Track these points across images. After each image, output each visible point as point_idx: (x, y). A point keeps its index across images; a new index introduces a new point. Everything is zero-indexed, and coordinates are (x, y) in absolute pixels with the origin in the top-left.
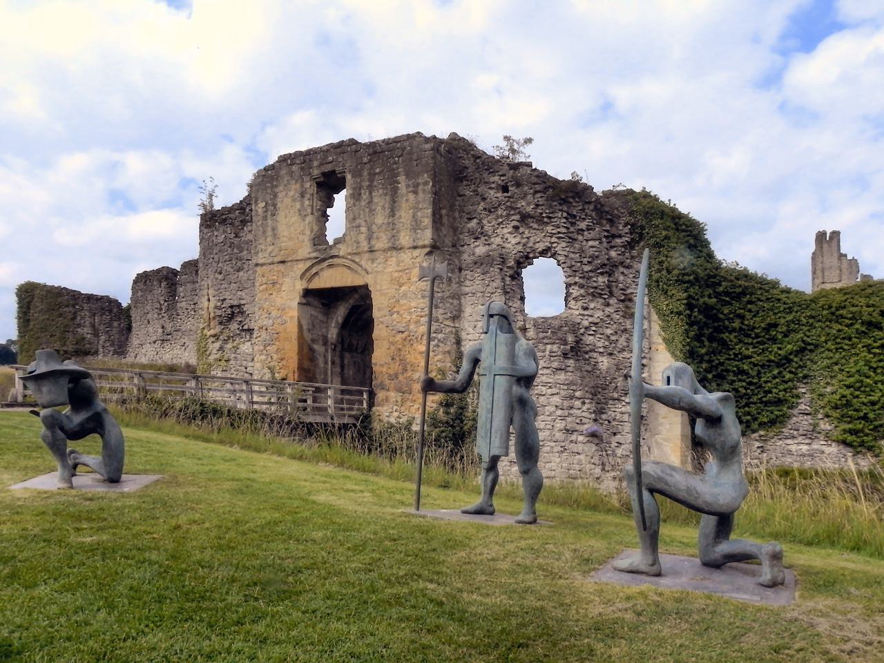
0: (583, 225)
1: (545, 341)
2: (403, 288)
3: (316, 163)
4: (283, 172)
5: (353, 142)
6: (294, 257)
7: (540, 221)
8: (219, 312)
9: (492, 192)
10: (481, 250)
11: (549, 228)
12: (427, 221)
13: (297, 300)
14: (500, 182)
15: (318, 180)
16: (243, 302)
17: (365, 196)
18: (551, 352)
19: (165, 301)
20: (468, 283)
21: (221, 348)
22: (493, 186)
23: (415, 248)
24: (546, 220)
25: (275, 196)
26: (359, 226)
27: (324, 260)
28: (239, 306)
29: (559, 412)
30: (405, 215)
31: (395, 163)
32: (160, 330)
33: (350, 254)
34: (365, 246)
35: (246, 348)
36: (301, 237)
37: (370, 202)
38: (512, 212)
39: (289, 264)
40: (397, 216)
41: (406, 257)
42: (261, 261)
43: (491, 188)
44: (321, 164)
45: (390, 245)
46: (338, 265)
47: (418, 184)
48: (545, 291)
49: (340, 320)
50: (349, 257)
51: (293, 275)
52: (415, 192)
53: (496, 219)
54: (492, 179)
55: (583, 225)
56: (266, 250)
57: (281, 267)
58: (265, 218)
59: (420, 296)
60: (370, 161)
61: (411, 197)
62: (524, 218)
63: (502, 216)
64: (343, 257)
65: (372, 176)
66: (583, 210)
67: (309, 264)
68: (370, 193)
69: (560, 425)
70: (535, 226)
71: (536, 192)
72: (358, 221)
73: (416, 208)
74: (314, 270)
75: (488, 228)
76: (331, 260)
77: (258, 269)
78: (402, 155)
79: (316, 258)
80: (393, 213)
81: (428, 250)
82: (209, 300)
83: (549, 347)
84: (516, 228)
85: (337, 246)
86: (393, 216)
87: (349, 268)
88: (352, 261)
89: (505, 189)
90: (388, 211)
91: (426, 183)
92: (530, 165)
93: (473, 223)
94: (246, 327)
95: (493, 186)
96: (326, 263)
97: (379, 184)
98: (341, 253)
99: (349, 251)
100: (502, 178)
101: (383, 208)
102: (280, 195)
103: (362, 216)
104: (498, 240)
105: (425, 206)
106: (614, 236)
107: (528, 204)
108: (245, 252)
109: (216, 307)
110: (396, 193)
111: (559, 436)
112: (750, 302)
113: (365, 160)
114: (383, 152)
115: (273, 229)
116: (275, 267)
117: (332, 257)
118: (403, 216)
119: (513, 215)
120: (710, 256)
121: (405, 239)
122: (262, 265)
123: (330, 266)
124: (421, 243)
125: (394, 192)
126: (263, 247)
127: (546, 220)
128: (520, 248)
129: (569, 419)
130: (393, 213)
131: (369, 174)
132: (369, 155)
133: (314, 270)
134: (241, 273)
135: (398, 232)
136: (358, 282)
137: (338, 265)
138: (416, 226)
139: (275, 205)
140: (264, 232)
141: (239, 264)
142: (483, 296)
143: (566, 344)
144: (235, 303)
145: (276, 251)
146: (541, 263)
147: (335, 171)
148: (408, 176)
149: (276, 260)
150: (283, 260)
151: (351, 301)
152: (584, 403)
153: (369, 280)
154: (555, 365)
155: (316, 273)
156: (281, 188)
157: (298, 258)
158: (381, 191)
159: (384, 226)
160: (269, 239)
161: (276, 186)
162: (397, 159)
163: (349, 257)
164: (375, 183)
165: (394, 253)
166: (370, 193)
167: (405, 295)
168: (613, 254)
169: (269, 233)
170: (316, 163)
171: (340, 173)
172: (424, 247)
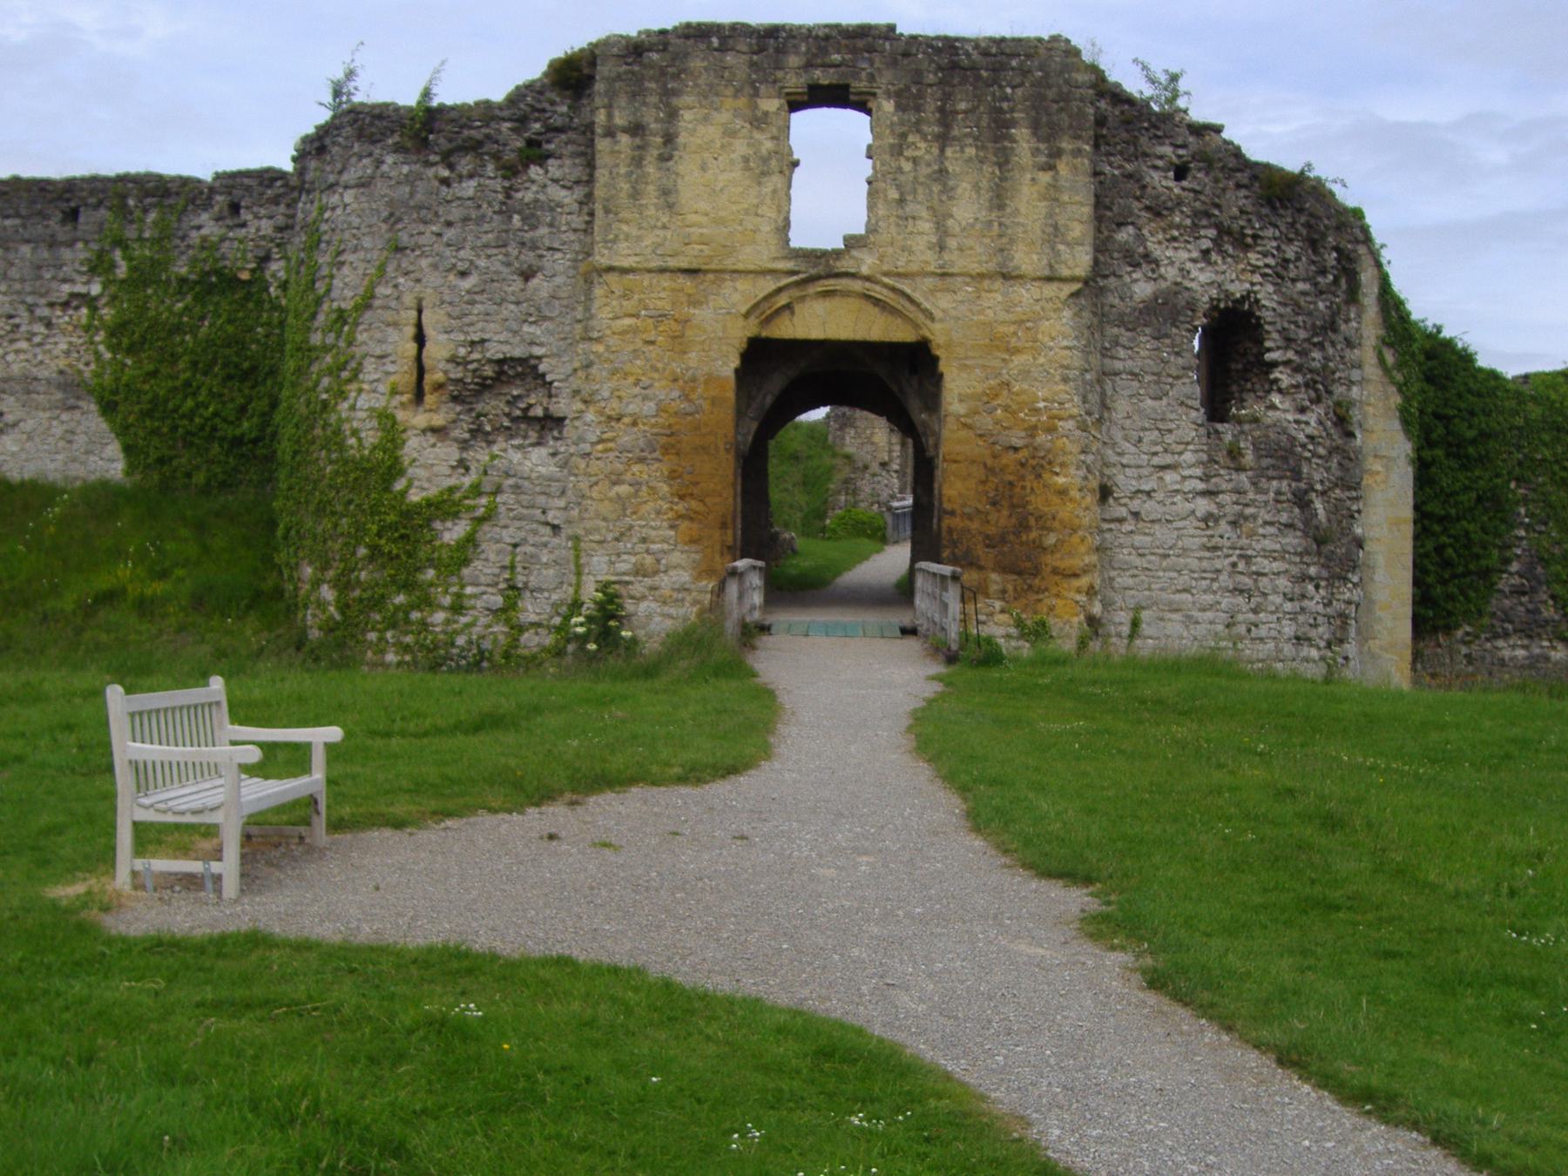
1: (1271, 473)
2: (1018, 360)
4: (697, 63)
6: (729, 263)
8: (457, 373)
9: (1156, 175)
14: (1174, 159)
15: (792, 98)
16: (537, 351)
18: (1278, 493)
20: (1122, 353)
22: (1160, 163)
23: (1049, 279)
24: (1249, 240)
25: (673, 114)
28: (522, 361)
29: (1288, 606)
31: (1006, 98)
33: (886, 274)
38: (1204, 222)
39: (711, 276)
40: (1008, 210)
41: (1026, 294)
43: (1155, 168)
45: (992, 266)
46: (846, 294)
49: (769, 400)
50: (886, 280)
51: (722, 303)
53: (1164, 230)
56: (639, 239)
57: (686, 283)
59: (1058, 378)
60: (941, 82)
63: (1178, 227)
64: (868, 279)
65: (946, 117)
66: (1292, 225)
67: (769, 285)
68: (942, 151)
69: (1289, 629)
70: (1231, 250)
73: (1052, 195)
74: (782, 300)
76: (831, 281)
77: (612, 278)
78: (1021, 85)
79: (793, 273)
80: (999, 199)
81: (1076, 286)
82: (420, 339)
83: (1275, 483)
84: (1206, 253)
85: (854, 253)
86: (1001, 207)
87: (877, 302)
88: (893, 289)
89: (1181, 173)
92: (1218, 130)
95: (1160, 163)
96: (819, 287)
97: (967, 135)
98: (865, 270)
99: (885, 268)
100: (1181, 152)
101: (976, 188)
102: (687, 115)
103: (920, 197)
105: (1077, 198)
109: (453, 360)
110: (1007, 162)
111: (1288, 649)
113: (931, 78)
114: (974, 68)
115: (665, 192)
116: (665, 281)
118: (1023, 210)
119: (1204, 227)
122: (625, 271)
124: (1066, 272)
125: (1004, 161)
127: (1249, 240)
128: (1214, 292)
129: (1301, 618)
130: (999, 199)
131: (941, 110)
132: (940, 68)
135: (1012, 241)
137: (846, 294)
139: (669, 139)
140: (635, 194)
141: (529, 257)
142: (1157, 383)
143: (1299, 480)
144: (518, 352)
147: (847, 87)
148: (1035, 127)
150: (695, 266)
152: (1317, 587)
153: (938, 334)
154: (1284, 518)
155: (788, 307)
156: (687, 99)
157: (740, 266)
158: (971, 151)
159: (978, 226)
161: (675, 93)
162: (1009, 90)
163: (886, 280)
164: (956, 132)
165: (998, 283)
166: (942, 151)
167: (1025, 373)
170: (794, 61)
171: (860, 93)
172: (1073, 279)
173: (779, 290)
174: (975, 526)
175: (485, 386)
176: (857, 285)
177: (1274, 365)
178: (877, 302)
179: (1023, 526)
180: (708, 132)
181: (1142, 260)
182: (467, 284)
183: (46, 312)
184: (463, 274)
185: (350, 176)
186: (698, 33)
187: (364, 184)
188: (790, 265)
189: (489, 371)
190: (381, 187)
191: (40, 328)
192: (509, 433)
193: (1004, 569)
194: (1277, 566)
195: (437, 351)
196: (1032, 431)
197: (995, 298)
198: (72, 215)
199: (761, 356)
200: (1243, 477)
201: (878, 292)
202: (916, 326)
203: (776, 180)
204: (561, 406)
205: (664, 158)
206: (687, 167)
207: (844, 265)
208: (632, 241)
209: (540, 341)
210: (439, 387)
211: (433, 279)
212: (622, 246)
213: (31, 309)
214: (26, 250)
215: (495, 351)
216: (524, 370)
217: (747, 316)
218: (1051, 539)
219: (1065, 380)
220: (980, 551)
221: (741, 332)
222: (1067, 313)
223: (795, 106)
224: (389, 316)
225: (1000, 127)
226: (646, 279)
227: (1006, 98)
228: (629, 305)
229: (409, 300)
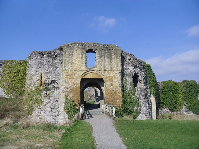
3: (87, 46)
4: (76, 47)
16: (56, 80)
17: (103, 57)
21: (46, 93)
25: (73, 52)
27: (89, 71)
28: (54, 81)
30: (113, 63)
34: (103, 69)
36: (82, 64)
37: (104, 59)
58: (68, 58)
65: (105, 53)
68: (104, 57)
69: (145, 110)
74: (86, 74)
91: (119, 57)
94: (56, 87)
98: (96, 70)
115: (72, 61)
117: (92, 71)
121: (114, 69)
123: (91, 73)
133: (86, 74)
139: (72, 55)
144: (54, 80)
150: (75, 69)
151: (88, 81)
156: (75, 51)
164: (106, 54)
176: (94, 72)
179: (115, 99)
184: (47, 70)
185: (33, 59)
187: (35, 60)
194: (143, 103)
195: (43, 80)
197: (111, 73)
199: (83, 80)
206: (74, 58)
208: (69, 67)
215: (50, 80)
220: (110, 102)
223: (87, 52)
225: (110, 54)
229: (40, 73)
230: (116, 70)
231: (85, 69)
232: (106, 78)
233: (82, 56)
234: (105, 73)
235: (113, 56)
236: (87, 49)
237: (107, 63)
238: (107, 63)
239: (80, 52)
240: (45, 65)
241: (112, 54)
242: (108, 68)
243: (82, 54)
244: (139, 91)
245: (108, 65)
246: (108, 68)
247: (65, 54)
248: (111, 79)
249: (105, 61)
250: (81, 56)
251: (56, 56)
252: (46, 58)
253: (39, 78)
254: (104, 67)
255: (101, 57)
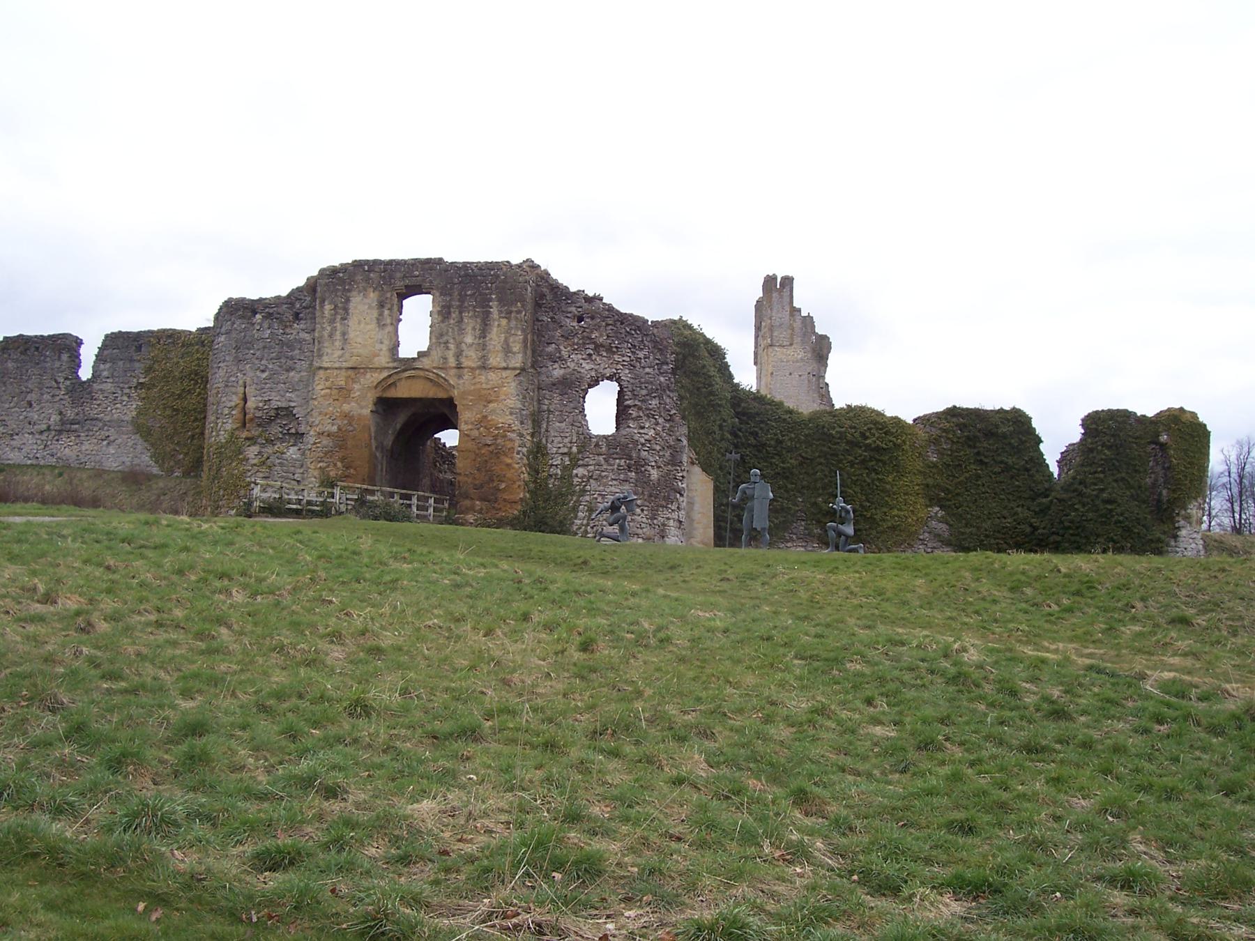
0: (641, 355)
2: (491, 405)
3: (398, 275)
4: (359, 278)
5: (440, 261)
7: (609, 349)
8: (259, 414)
10: (558, 372)
11: (616, 357)
12: (516, 347)
13: (371, 407)
19: (66, 379)
23: (505, 369)
25: (348, 300)
26: (447, 342)
30: (496, 337)
31: (488, 288)
32: (55, 418)
34: (452, 362)
35: (292, 453)
36: (378, 346)
37: (461, 321)
42: (325, 365)
44: (405, 276)
47: (511, 312)
48: (600, 410)
49: (398, 426)
52: (509, 319)
54: (570, 309)
55: (641, 355)
57: (350, 372)
58: (332, 321)
61: (504, 322)
62: (598, 347)
65: (462, 299)
67: (385, 374)
68: (461, 313)
71: (608, 325)
72: (445, 338)
73: (508, 332)
75: (564, 353)
77: (321, 372)
80: (483, 334)
90: (478, 332)
93: (551, 348)
94: (293, 431)
96: (407, 374)
101: (474, 329)
104: (572, 365)
106: (663, 363)
107: (601, 335)
108: (297, 352)
109: (257, 408)
112: (762, 422)
115: (344, 334)
116: (343, 373)
120: (731, 377)
121: (496, 360)
122: (326, 369)
125: (487, 315)
126: (329, 351)
131: (460, 295)
134: (292, 374)
136: (442, 395)
137: (419, 377)
138: (507, 350)
139: (346, 310)
140: (331, 336)
141: (290, 363)
144: (284, 405)
145: (347, 355)
146: (605, 384)
148: (500, 300)
149: (345, 365)
156: (354, 293)
160: (337, 343)
167: (493, 411)
168: (662, 379)
169: (338, 336)
172: (515, 369)
173: (390, 376)
174: (470, 480)
175: (271, 420)
176: (421, 373)
177: (629, 407)
178: (431, 380)
180: (363, 305)
181: (557, 359)
182: (264, 375)
183: (127, 391)
184: (263, 371)
185: (223, 330)
186: (358, 264)
188: (395, 364)
189: (272, 413)
190: (234, 335)
191: (125, 398)
192: (282, 440)
193: (482, 499)
195: (251, 404)
196: (496, 437)
198: (139, 348)
200: (601, 458)
201: (431, 376)
202: (446, 390)
203: (389, 328)
204: (302, 429)
205: (344, 319)
206: (352, 322)
207: (418, 365)
208: (331, 356)
209: (293, 399)
210: (252, 420)
211: (251, 374)
212: (325, 358)
213: (122, 389)
214: (121, 363)
215: (274, 404)
216: (285, 413)
217: (376, 387)
218: (503, 486)
219: (511, 414)
221: (371, 397)
222: (513, 384)
224: (234, 390)
225: (484, 303)
226: (336, 372)
227: (488, 288)
228: (328, 384)
229: (241, 382)
230: (504, 365)
231: (391, 365)
232: (464, 394)
233: (381, 314)
234: (460, 377)
235: (494, 311)
236: (400, 284)
237: (469, 339)
238: (469, 339)
239: (373, 296)
240: (258, 353)
241: (491, 300)
242: (471, 358)
243: (381, 305)
244: (604, 449)
245: (471, 345)
246: (471, 358)
247: (322, 307)
248: (486, 398)
249: (461, 331)
250: (375, 313)
251: (297, 317)
252: (261, 324)
253: (236, 400)
254: (458, 355)
255: (449, 313)
